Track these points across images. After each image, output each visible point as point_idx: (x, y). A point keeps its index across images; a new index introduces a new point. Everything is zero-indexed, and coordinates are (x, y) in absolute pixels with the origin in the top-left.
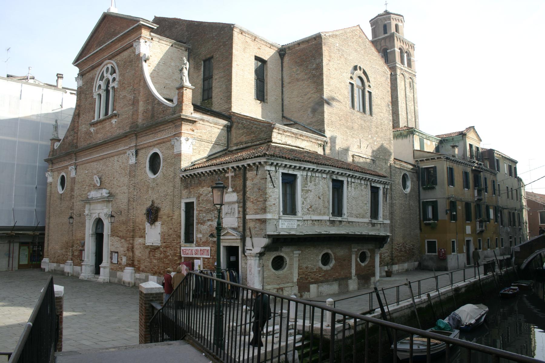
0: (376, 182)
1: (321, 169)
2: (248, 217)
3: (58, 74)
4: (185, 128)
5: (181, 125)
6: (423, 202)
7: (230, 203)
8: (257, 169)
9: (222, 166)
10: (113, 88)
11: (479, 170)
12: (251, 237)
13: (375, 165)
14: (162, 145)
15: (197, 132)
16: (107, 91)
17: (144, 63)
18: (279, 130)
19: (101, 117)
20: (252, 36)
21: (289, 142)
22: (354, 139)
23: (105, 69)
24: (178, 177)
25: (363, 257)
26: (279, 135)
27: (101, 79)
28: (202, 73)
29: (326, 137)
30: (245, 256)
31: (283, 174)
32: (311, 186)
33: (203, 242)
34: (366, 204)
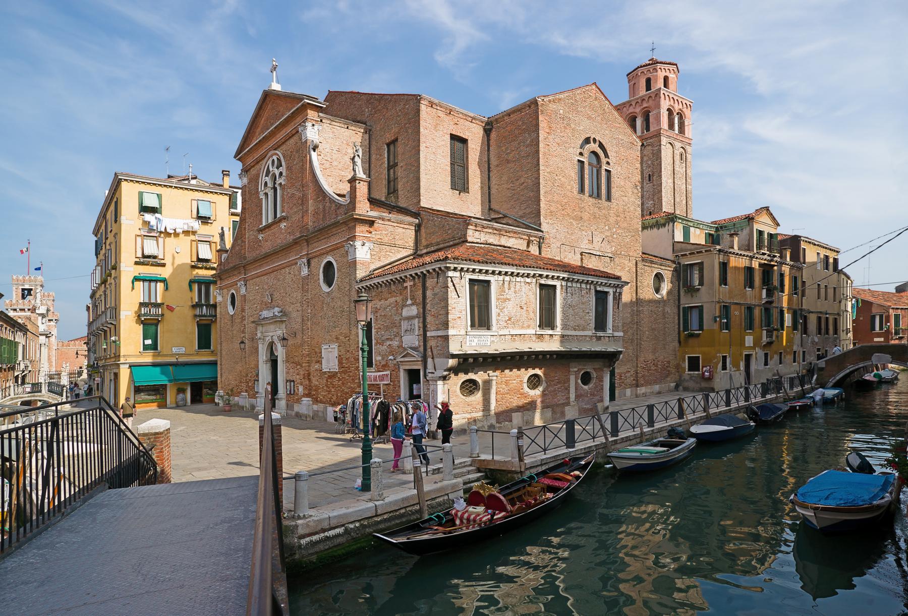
0: (603, 286)
1: (523, 272)
2: (429, 334)
3: (223, 171)
4: (361, 230)
5: (355, 226)
6: (684, 308)
7: (409, 318)
8: (438, 276)
9: (399, 274)
10: (280, 184)
11: (772, 263)
12: (433, 358)
13: (614, 264)
14: (335, 252)
15: (376, 234)
16: (275, 189)
17: (312, 152)
18: (476, 226)
19: (270, 221)
20: (446, 109)
21: (491, 241)
22: (583, 232)
23: (270, 162)
24: (354, 290)
25: (586, 379)
26: (477, 232)
27: (267, 175)
28: (386, 159)
29: (542, 232)
30: (428, 380)
31: (470, 280)
32: (510, 294)
33: (382, 366)
34: (588, 313)
